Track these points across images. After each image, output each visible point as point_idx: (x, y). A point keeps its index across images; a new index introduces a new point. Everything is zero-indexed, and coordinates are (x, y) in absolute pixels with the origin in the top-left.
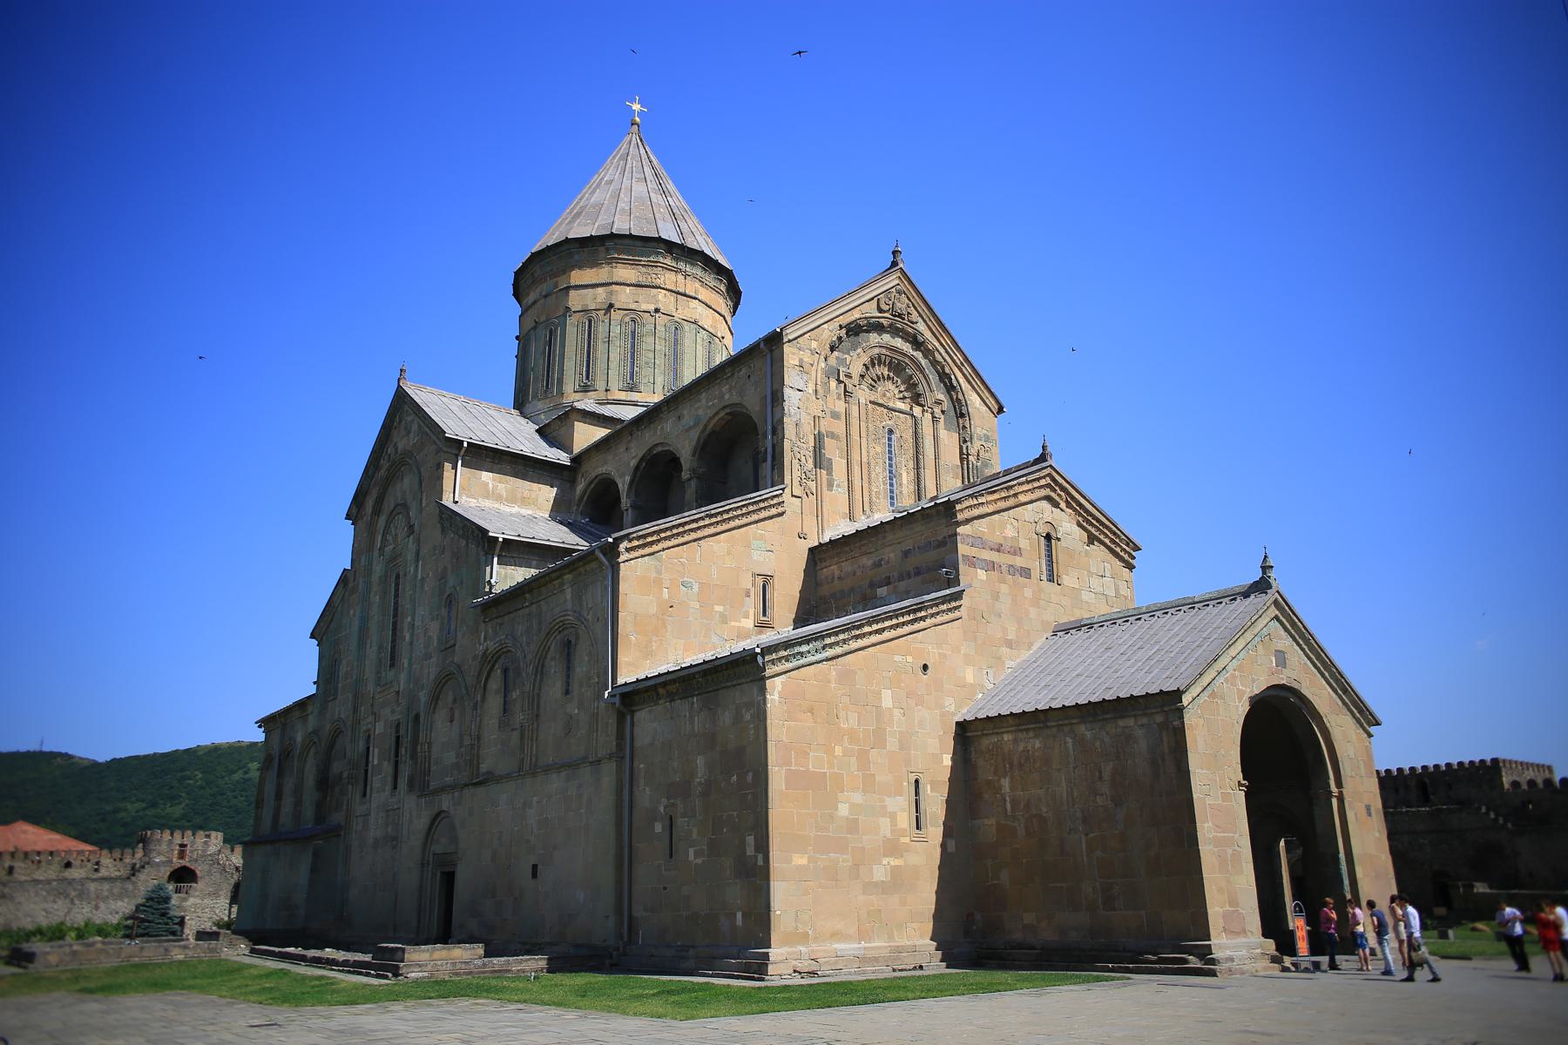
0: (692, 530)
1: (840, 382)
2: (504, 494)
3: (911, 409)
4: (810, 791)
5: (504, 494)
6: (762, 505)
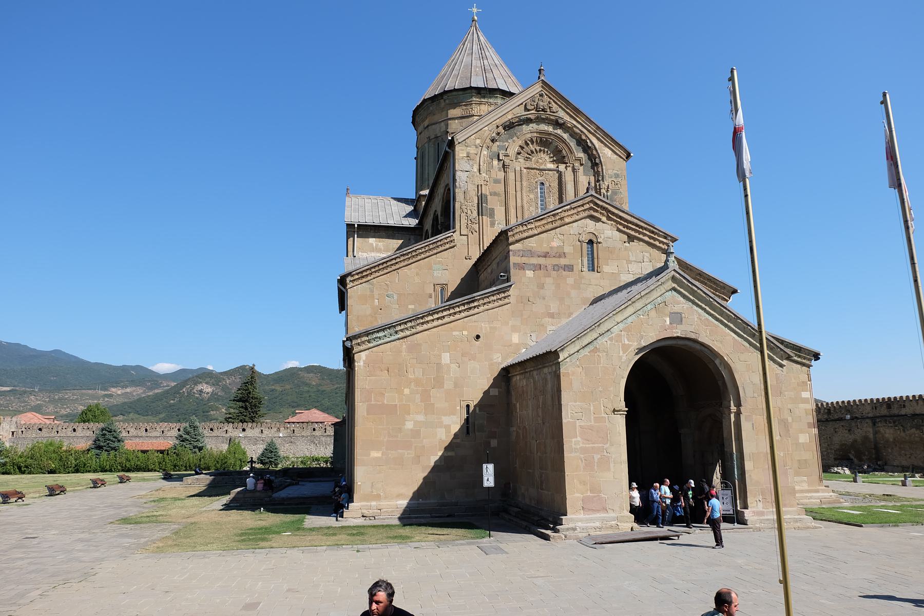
0: (392, 265)
1: (499, 160)
2: (383, 248)
3: (558, 167)
4: (384, 416)
5: (383, 248)
6: (439, 243)
